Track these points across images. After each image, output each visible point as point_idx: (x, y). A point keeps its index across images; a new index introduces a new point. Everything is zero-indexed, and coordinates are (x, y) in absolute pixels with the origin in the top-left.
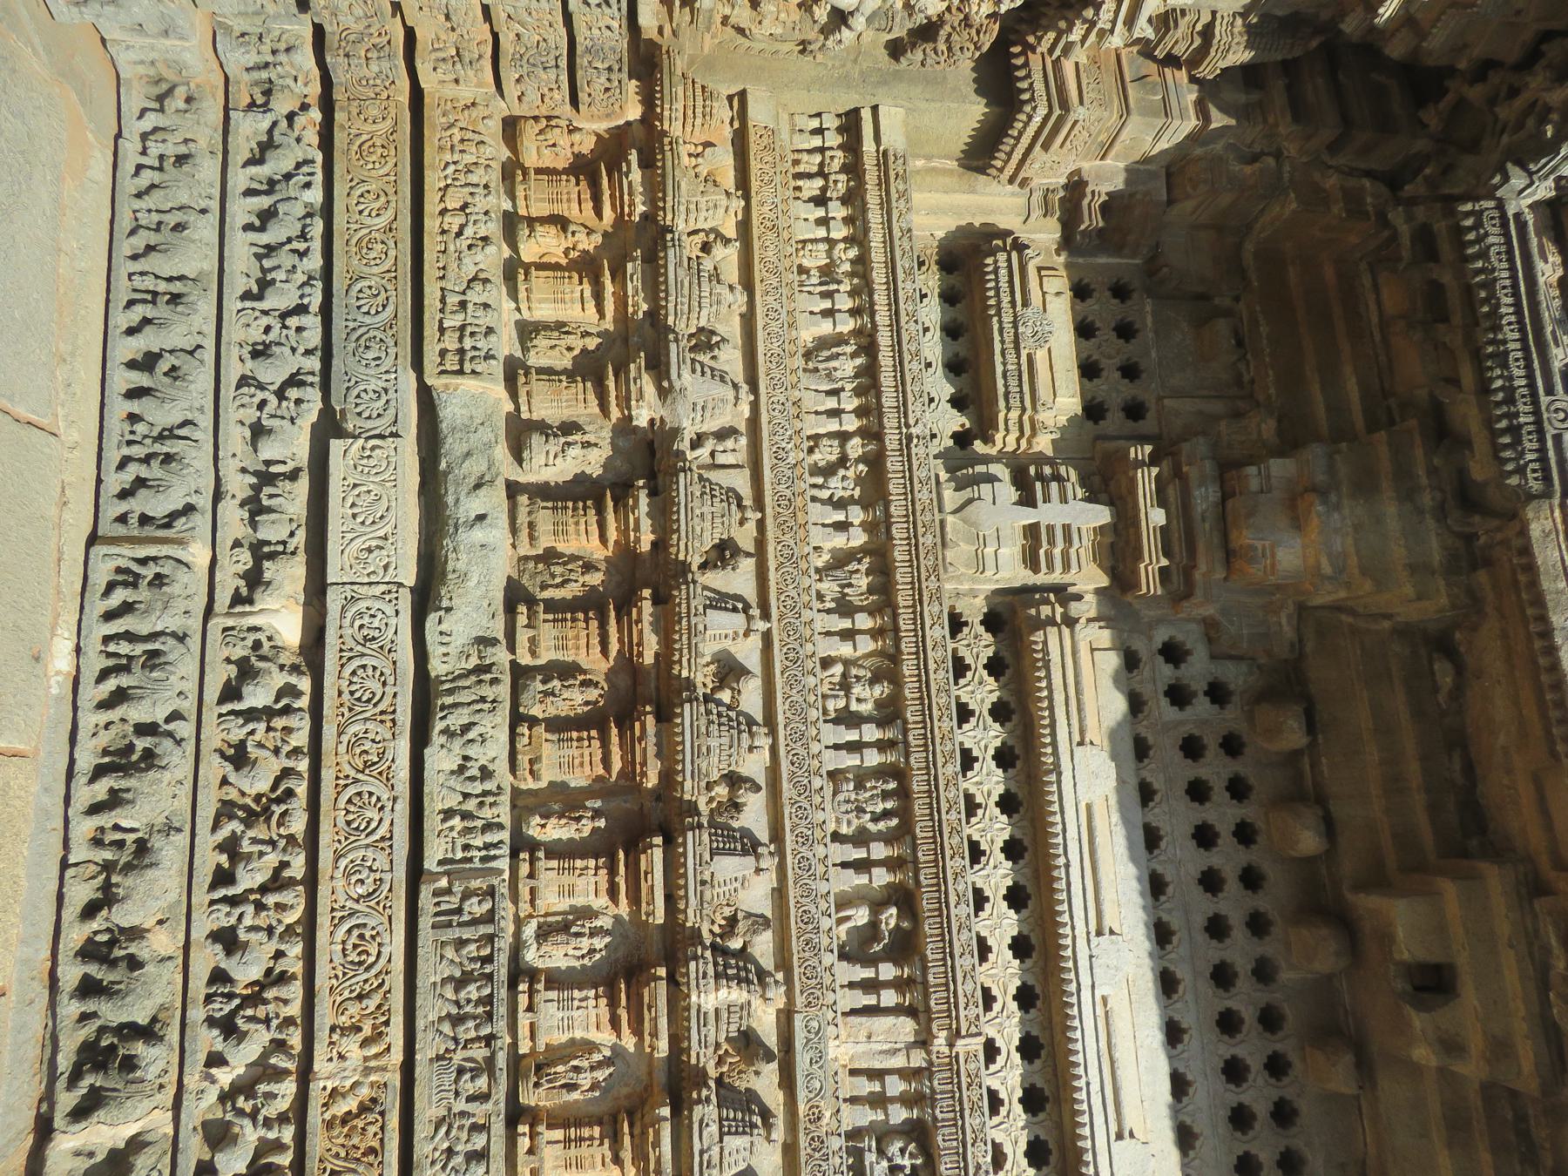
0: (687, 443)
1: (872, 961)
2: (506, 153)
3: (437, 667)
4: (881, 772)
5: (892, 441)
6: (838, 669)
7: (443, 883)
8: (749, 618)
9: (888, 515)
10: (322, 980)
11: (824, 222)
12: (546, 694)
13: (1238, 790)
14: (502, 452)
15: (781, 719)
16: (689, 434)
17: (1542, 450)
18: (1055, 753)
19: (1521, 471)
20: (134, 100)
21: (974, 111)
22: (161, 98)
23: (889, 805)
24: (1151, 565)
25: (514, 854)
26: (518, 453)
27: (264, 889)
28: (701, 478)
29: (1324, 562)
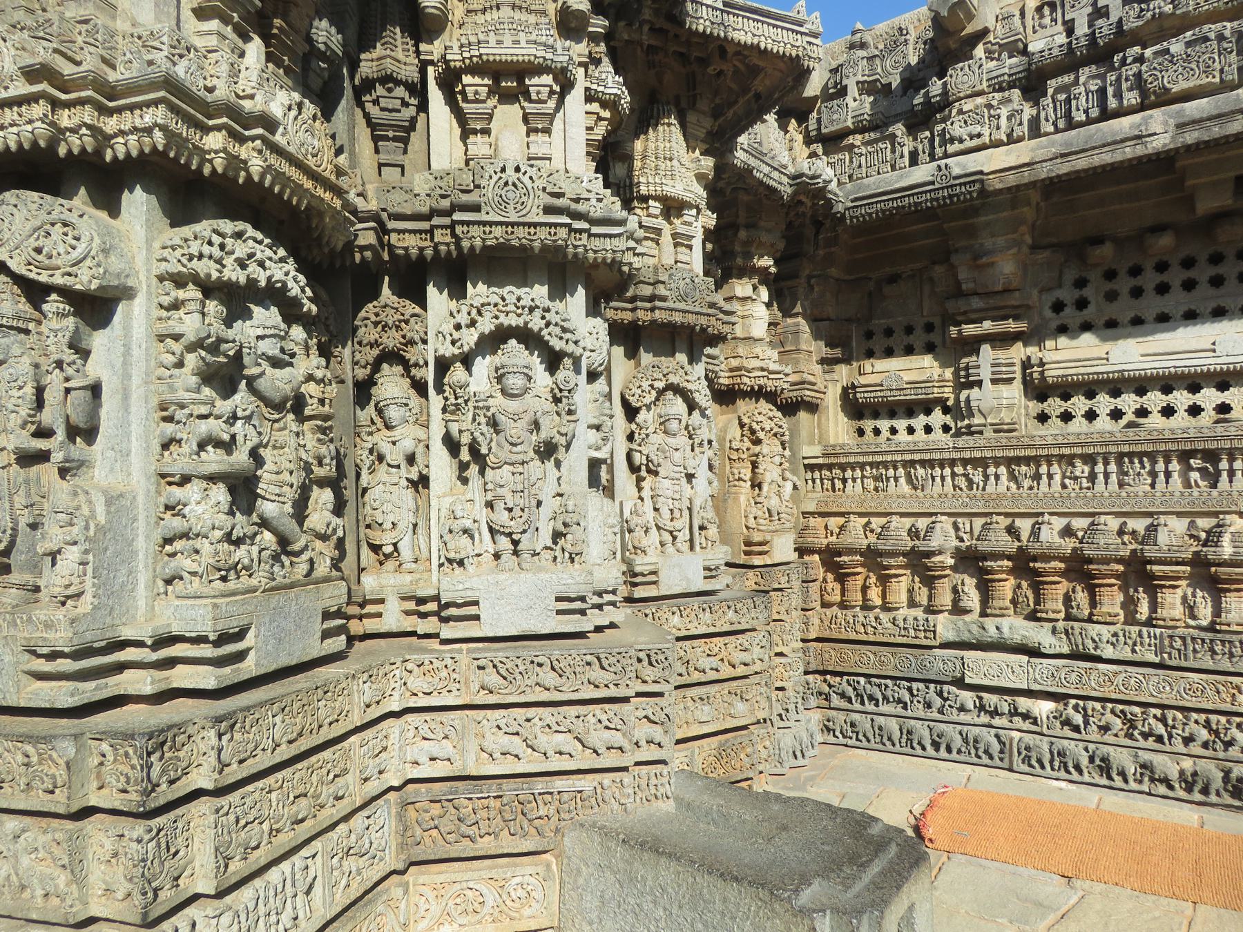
1: (1218, 473)
3: (1066, 650)
4: (1120, 463)
5: (956, 455)
6: (1067, 481)
7: (1166, 656)
8: (1043, 523)
10: (1210, 706)
11: (854, 480)
13: (1136, 271)
14: (967, 618)
16: (956, 543)
17: (960, 185)
18: (1113, 372)
19: (970, 193)
20: (831, 739)
21: (803, 415)
22: (829, 730)
23: (1136, 461)
24: (1012, 326)
25: (1155, 626)
26: (967, 611)
27: (1166, 725)
28: (978, 539)
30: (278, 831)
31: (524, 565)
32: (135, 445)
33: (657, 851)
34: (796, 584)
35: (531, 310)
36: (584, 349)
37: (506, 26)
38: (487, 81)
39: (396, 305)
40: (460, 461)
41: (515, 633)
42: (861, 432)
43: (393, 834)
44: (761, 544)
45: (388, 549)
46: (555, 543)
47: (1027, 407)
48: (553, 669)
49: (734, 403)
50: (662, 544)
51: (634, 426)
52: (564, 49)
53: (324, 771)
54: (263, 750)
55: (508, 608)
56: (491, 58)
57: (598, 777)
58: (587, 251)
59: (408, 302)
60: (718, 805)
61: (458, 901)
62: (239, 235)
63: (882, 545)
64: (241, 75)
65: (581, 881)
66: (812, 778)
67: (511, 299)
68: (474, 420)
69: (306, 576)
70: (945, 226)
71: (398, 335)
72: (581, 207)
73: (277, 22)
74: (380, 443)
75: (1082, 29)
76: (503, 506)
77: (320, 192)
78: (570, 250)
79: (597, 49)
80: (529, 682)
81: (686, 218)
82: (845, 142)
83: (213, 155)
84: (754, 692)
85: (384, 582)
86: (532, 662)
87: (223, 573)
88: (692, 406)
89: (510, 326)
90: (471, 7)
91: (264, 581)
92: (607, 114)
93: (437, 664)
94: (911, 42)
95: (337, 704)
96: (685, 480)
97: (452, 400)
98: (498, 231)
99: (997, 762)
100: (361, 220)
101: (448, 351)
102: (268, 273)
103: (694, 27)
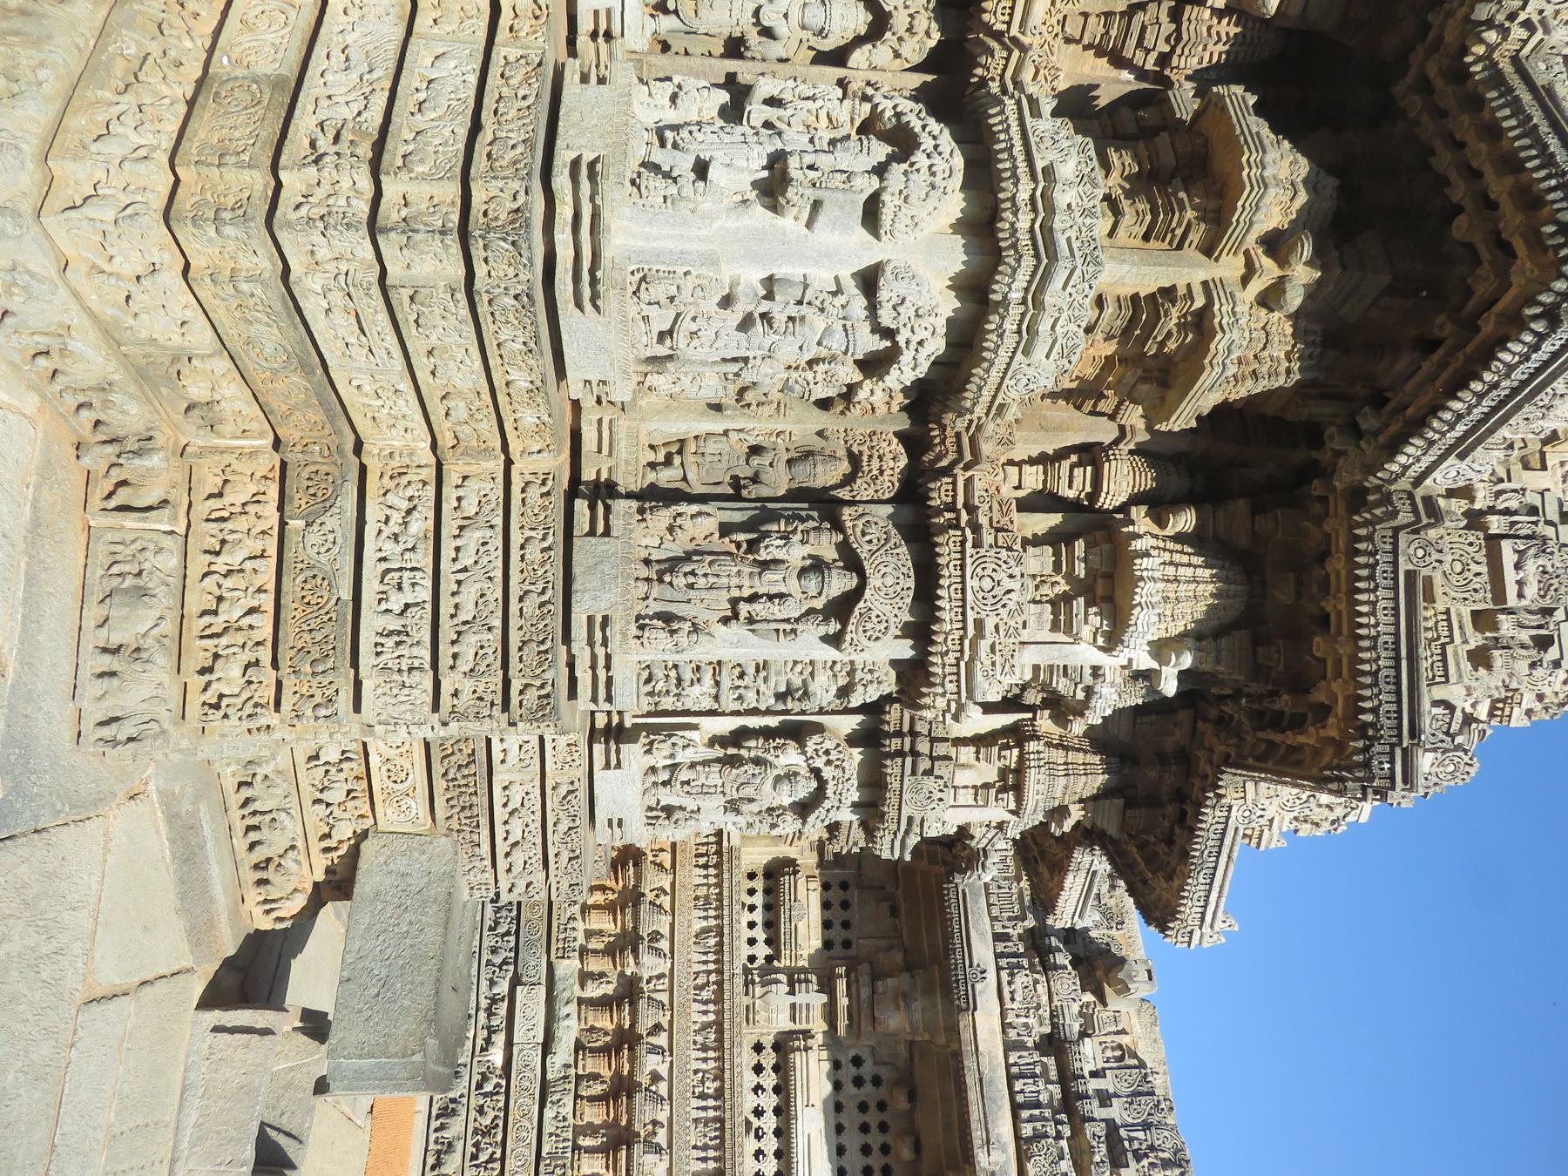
3: (550, 1076)
4: (715, 1119)
5: (726, 976)
6: (700, 1074)
11: (706, 876)
13: (883, 1127)
14: (577, 987)
16: (646, 977)
19: (959, 999)
24: (842, 1023)
25: (573, 1151)
26: (582, 986)
27: (487, 1162)
32: (742, 651)
38: (1013, 766)
41: (596, 791)
42: (752, 876)
75: (1094, 1085)
94: (1110, 932)
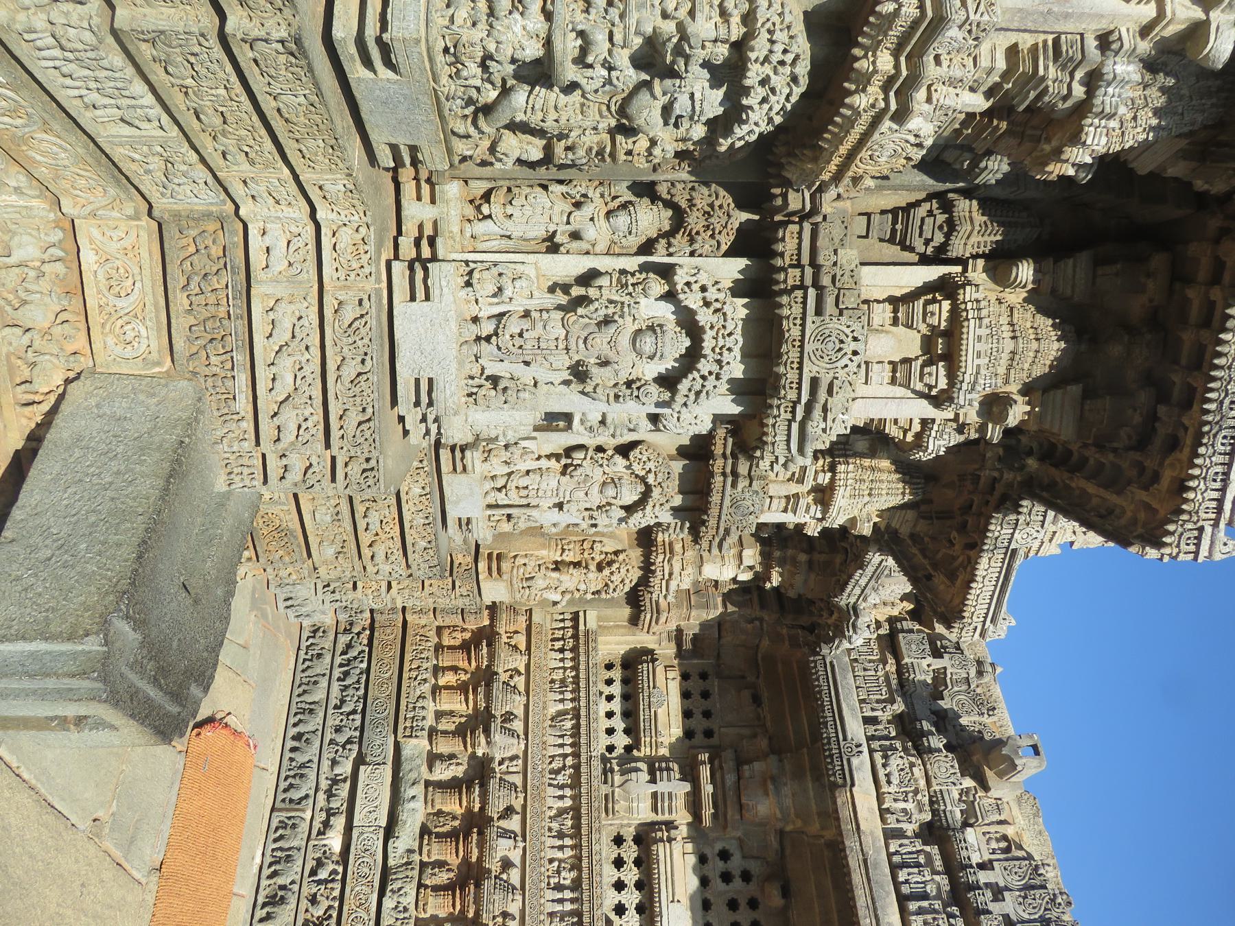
0: (497, 763)
2: (437, 640)
3: (391, 862)
4: (572, 913)
5: (583, 758)
6: (556, 864)
9: (580, 793)
11: (562, 660)
12: (432, 874)
14: (424, 768)
15: (527, 886)
16: (498, 758)
17: (842, 765)
18: (660, 907)
19: (834, 774)
20: (305, 635)
21: (627, 611)
22: (315, 632)
24: (707, 812)
26: (430, 769)
28: (501, 779)
29: (778, 812)
30: (186, 93)
31: (465, 347)
33: (171, 476)
34: (460, 603)
35: (719, 362)
36: (679, 412)
37: (995, 345)
38: (943, 324)
39: (729, 226)
40: (571, 286)
42: (609, 667)
43: (189, 207)
44: (499, 569)
45: (485, 209)
46: (488, 378)
47: (629, 825)
48: (359, 374)
49: (639, 545)
50: (493, 478)
51: (610, 452)
52: (971, 400)
53: (252, 142)
54: (269, 84)
55: (423, 331)
56: (965, 330)
57: (250, 416)
58: (775, 417)
59: (732, 238)
60: (222, 536)
61: (122, 271)
62: (794, 79)
63: (497, 687)
64: (951, 89)
65: (142, 397)
66: (265, 616)
67: (729, 342)
68: (611, 302)
69: (452, 131)
70: (805, 750)
71: (699, 227)
72: (817, 413)
73: (1004, 125)
74: (594, 205)
75: (983, 877)
76: (525, 328)
77: (836, 161)
78: (776, 402)
79: (972, 431)
80: (345, 350)
81: (813, 508)
82: (889, 656)
83: (871, 59)
84: (345, 565)
85: (452, 204)
86: (366, 354)
87: (452, 50)
88: (629, 509)
89: (703, 341)
90: (1015, 311)
91: (446, 90)
92: (909, 438)
93: (365, 258)
95: (321, 158)
96: (557, 501)
97: (631, 280)
98: (796, 332)
99: (281, 797)
100: (812, 196)
101: (680, 278)
102: (756, 107)
103: (993, 521)
